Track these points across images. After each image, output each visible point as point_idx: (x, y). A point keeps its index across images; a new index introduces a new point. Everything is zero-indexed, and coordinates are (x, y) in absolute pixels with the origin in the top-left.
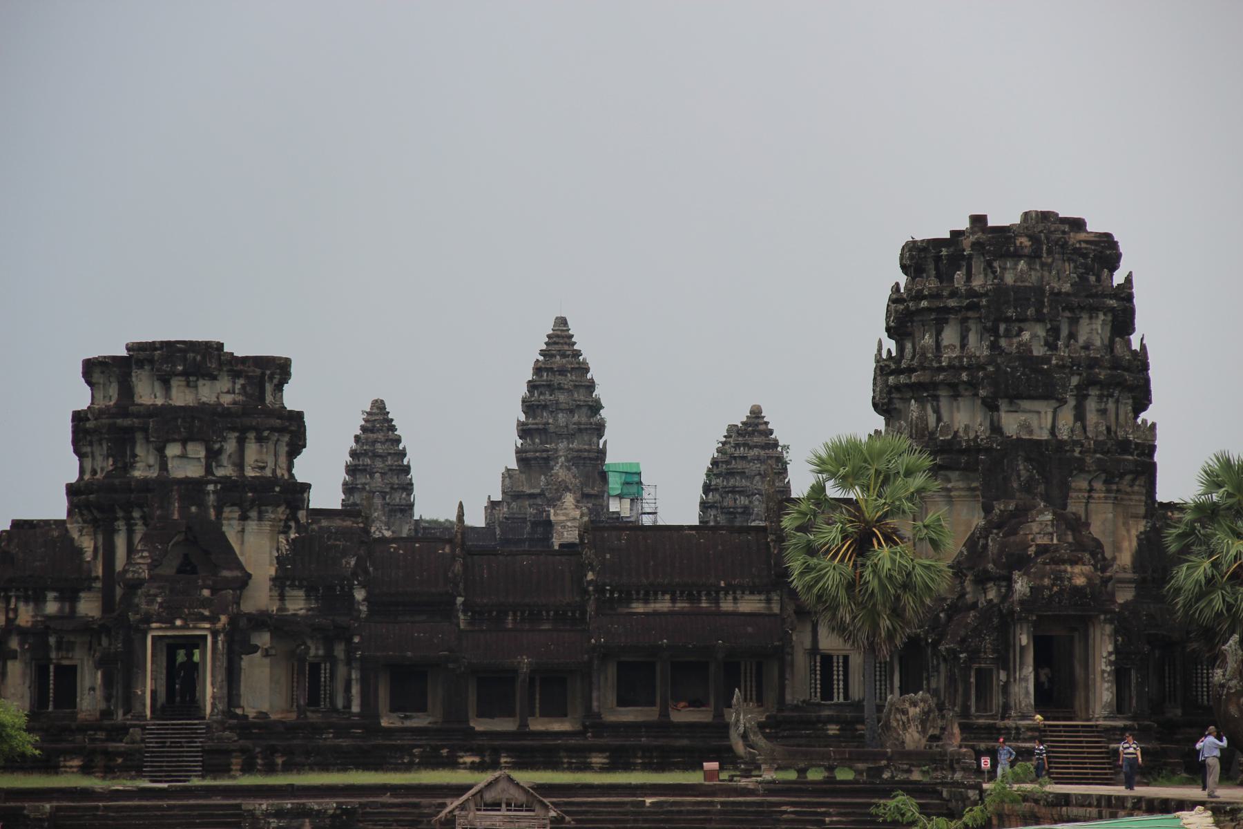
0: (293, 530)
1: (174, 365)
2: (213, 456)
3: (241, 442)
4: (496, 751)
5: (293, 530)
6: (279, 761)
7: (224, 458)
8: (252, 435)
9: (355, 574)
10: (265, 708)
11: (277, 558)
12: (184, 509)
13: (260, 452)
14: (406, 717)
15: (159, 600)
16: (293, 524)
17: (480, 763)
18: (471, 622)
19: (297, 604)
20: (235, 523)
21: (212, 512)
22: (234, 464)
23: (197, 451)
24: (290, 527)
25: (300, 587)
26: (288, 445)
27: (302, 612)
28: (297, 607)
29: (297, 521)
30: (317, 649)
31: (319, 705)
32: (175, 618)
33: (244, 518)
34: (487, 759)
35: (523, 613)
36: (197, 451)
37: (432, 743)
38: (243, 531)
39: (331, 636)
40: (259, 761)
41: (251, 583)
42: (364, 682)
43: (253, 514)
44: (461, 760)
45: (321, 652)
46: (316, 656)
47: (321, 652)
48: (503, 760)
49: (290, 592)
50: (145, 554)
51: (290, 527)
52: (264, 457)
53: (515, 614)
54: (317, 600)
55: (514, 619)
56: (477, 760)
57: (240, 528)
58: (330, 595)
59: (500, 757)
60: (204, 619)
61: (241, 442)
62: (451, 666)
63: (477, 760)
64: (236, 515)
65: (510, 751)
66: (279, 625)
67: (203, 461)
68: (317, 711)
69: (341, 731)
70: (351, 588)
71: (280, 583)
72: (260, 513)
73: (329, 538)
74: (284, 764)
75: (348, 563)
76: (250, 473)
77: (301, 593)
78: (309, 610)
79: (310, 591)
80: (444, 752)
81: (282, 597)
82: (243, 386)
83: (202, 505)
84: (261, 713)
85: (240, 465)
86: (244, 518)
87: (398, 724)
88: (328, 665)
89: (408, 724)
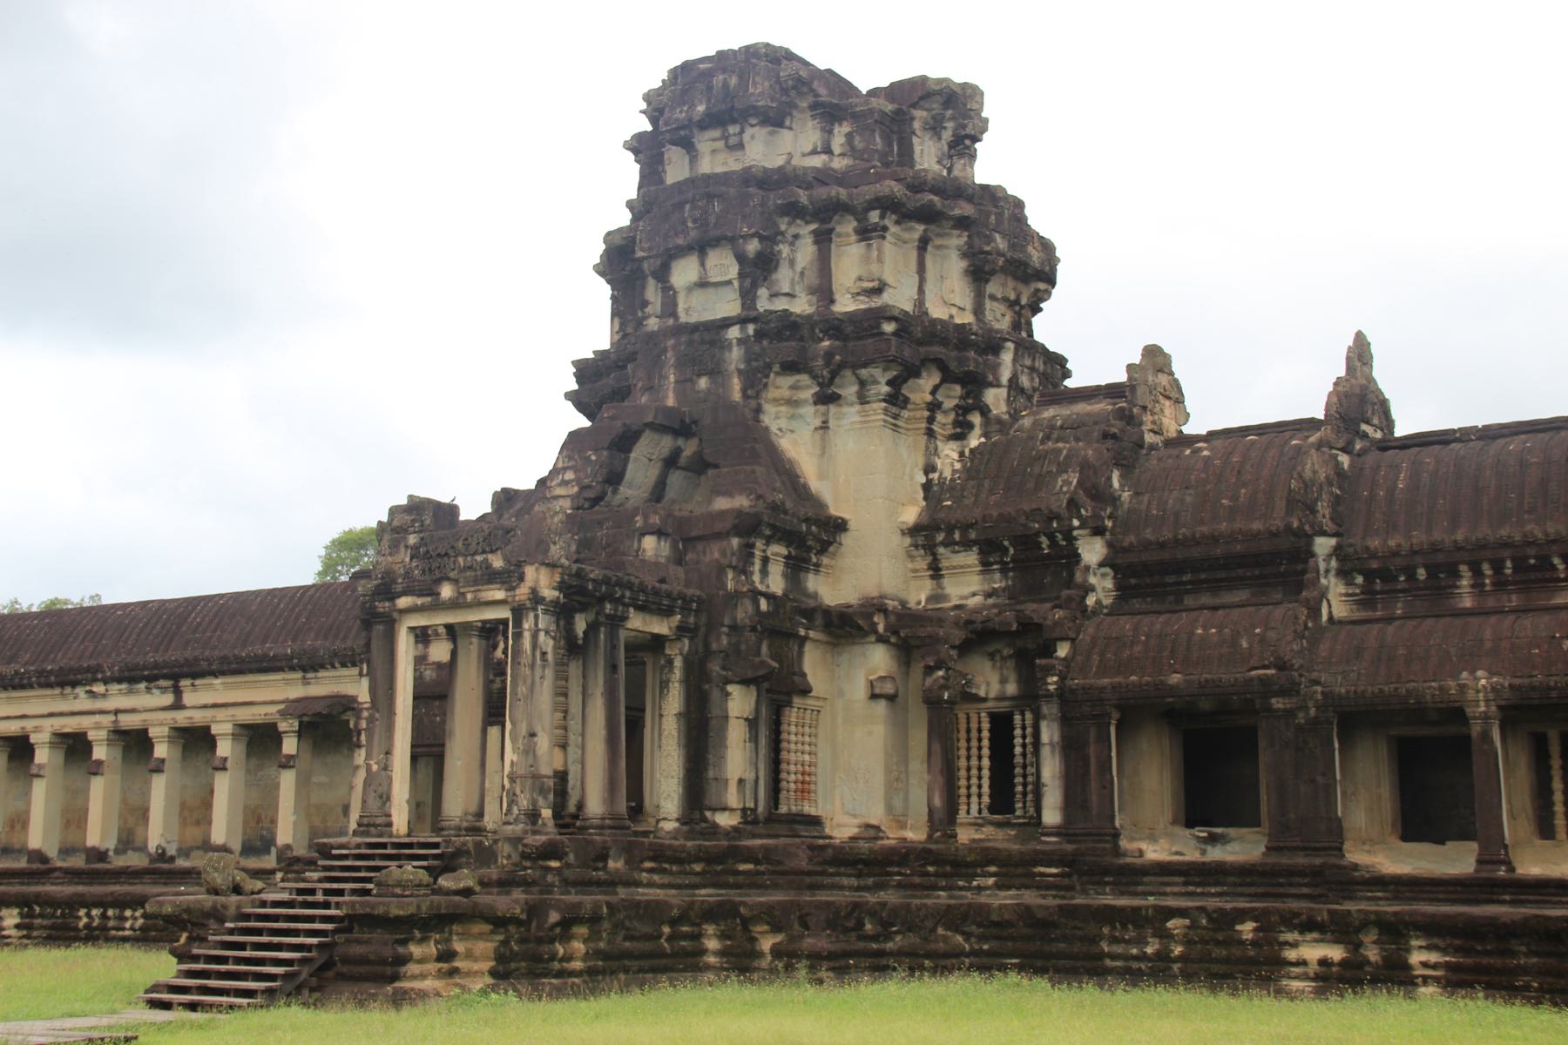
0: (977, 431)
1: (693, 106)
2: (758, 270)
3: (823, 239)
4: (1395, 932)
5: (977, 431)
6: (766, 944)
7: (784, 278)
8: (847, 226)
9: (1073, 504)
10: (877, 815)
11: (927, 487)
12: (684, 382)
13: (866, 260)
14: (1213, 839)
15: (412, 539)
16: (976, 419)
17: (1343, 963)
18: (1366, 599)
19: (967, 585)
20: (809, 410)
21: (736, 384)
22: (812, 291)
23: (723, 264)
24: (971, 426)
25: (966, 545)
26: (964, 255)
27: (978, 599)
28: (967, 591)
29: (984, 411)
30: (1003, 681)
31: (1012, 811)
32: (439, 581)
33: (827, 398)
34: (1373, 954)
35: (1498, 567)
36: (723, 264)
37: (1213, 903)
38: (824, 426)
39: (1024, 644)
40: (712, 944)
41: (846, 539)
42: (1071, 748)
43: (849, 390)
44: (1291, 955)
45: (1012, 688)
46: (999, 699)
47: (1012, 688)
48: (1416, 958)
49: (949, 559)
50: (569, 476)
51: (971, 426)
52: (874, 268)
53: (1477, 573)
54: (1004, 571)
55: (1477, 585)
56: (1336, 953)
57: (818, 423)
58: (1030, 556)
59: (1408, 950)
60: (492, 577)
61: (823, 239)
62: (1277, 703)
63: (1336, 953)
64: (808, 394)
65: (1434, 930)
66: (910, 634)
67: (736, 284)
68: (1007, 824)
69: (1014, 869)
70: (1071, 539)
71: (928, 537)
72: (862, 384)
73: (1047, 438)
74: (777, 952)
75: (1069, 483)
76: (845, 304)
77: (971, 558)
78: (988, 595)
79: (989, 551)
80: (1247, 929)
81: (936, 572)
82: (849, 136)
83: (716, 372)
84: (868, 826)
85: (825, 293)
86: (827, 398)
87: (1192, 855)
88: (1028, 716)
89: (1216, 854)
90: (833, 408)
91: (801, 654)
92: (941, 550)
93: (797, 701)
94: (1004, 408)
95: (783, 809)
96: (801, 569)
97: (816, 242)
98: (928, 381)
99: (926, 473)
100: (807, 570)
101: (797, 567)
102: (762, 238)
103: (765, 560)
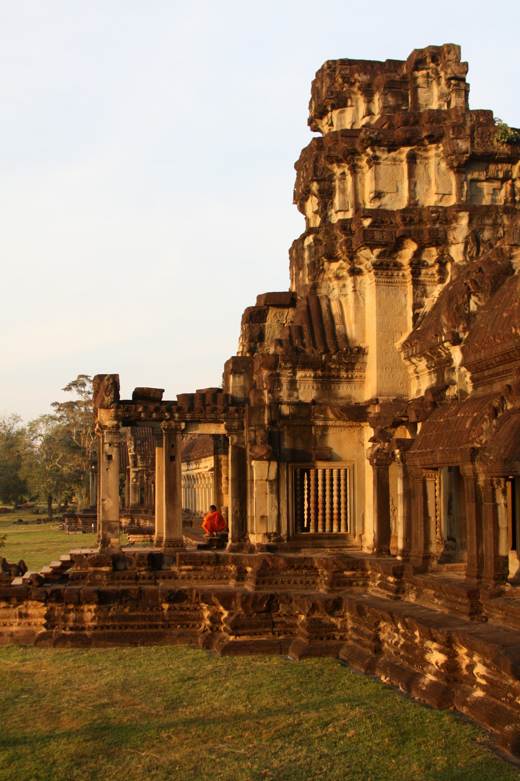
3: (354, 170)
7: (337, 200)
90: (359, 278)
91: (324, 436)
92: (414, 360)
93: (321, 465)
94: (461, 258)
95: (312, 531)
96: (333, 383)
97: (352, 174)
98: (410, 249)
99: (414, 310)
100: (339, 382)
101: (327, 381)
102: (318, 182)
103: (293, 383)
